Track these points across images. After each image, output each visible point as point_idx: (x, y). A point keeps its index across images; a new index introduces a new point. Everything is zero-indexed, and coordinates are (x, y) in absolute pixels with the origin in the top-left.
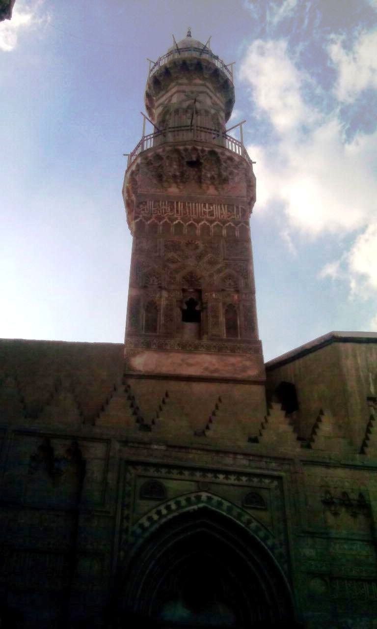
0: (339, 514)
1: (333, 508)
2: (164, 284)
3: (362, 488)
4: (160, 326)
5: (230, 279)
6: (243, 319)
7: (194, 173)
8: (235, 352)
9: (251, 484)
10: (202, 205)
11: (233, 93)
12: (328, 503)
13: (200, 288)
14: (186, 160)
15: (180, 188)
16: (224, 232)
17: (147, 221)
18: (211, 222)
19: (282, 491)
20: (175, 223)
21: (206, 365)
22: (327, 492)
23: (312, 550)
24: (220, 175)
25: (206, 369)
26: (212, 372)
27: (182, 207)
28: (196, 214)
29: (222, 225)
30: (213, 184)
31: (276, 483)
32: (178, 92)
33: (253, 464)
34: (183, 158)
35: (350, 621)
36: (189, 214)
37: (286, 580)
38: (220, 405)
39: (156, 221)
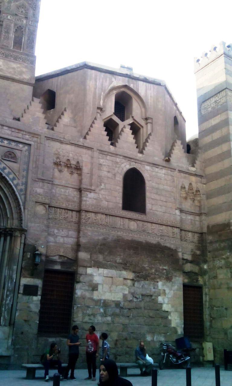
0: (63, 172)
1: (60, 168)
3: (80, 158)
5: (23, 8)
6: (26, 38)
8: (16, 60)
9: (10, 146)
12: (57, 164)
19: (30, 153)
22: (58, 158)
23: (41, 190)
31: (26, 147)
33: (14, 134)
35: (56, 231)
37: (21, 204)
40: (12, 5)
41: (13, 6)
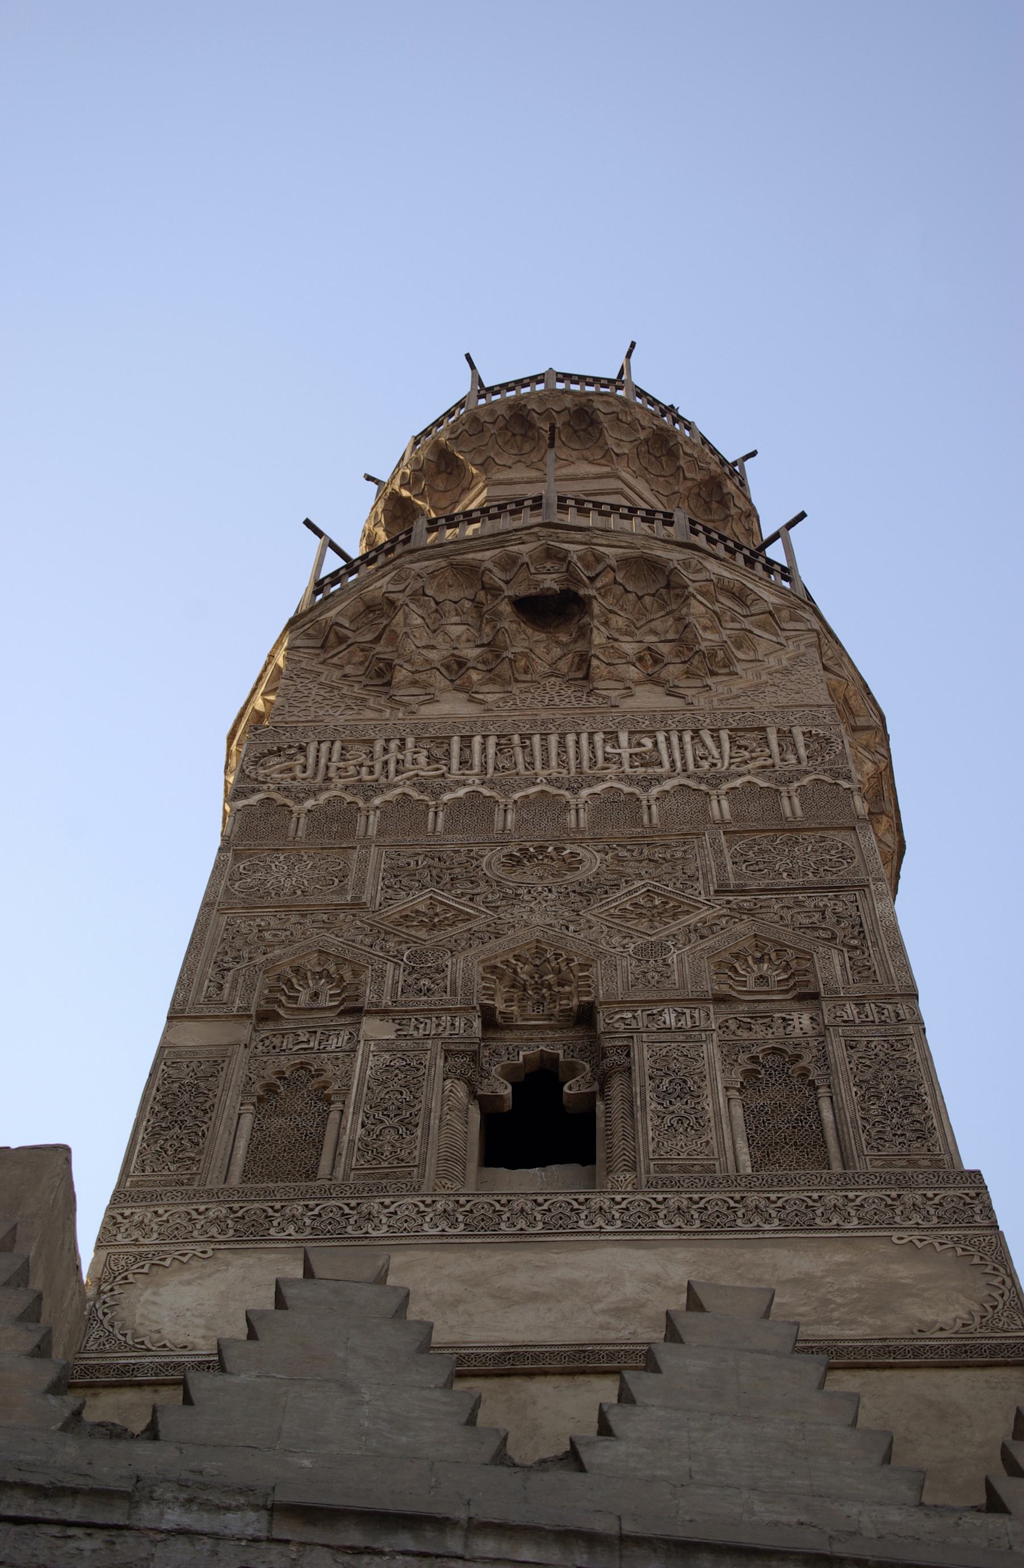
10: (599, 738)
15: (482, 702)
21: (630, 1289)
28: (563, 763)
30: (652, 680)
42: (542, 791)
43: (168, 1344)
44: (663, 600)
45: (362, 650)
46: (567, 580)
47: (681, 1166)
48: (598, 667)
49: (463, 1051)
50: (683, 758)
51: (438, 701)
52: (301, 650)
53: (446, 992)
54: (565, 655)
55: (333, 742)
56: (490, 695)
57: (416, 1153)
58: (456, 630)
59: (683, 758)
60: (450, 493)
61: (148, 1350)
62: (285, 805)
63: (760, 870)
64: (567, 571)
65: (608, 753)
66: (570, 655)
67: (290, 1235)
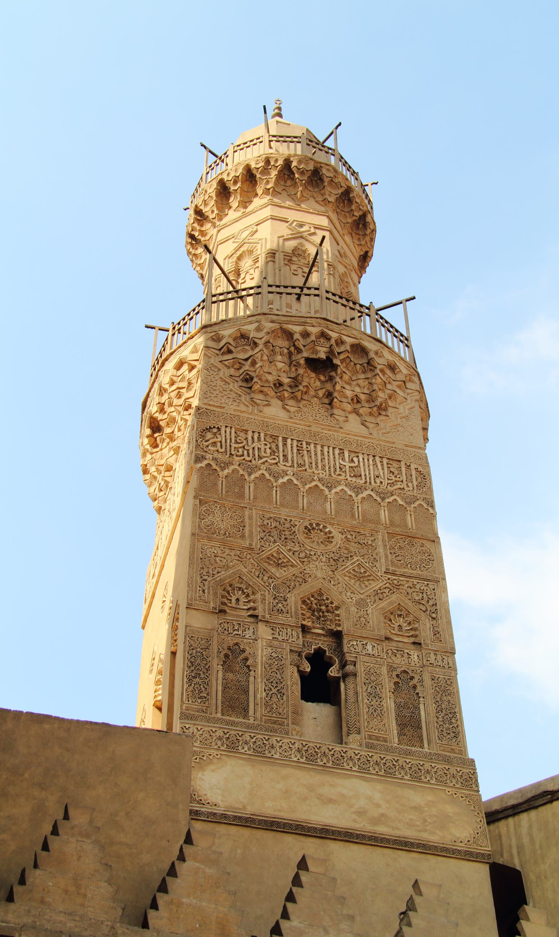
2: (260, 612)
4: (256, 704)
6: (432, 708)
7: (318, 383)
10: (337, 451)
11: (372, 240)
13: (339, 629)
14: (305, 354)
15: (288, 411)
16: (384, 515)
17: (223, 469)
18: (358, 489)
20: (281, 481)
21: (362, 803)
24: (371, 399)
25: (361, 813)
26: (376, 821)
27: (295, 451)
28: (323, 469)
29: (379, 499)
30: (356, 412)
32: (273, 218)
34: (299, 351)
36: (311, 467)
38: (418, 900)
39: (241, 472)
40: (370, 611)
41: (372, 613)
42: (316, 485)
43: (210, 803)
44: (365, 369)
45: (239, 363)
46: (329, 352)
47: (376, 736)
48: (336, 402)
49: (296, 651)
50: (369, 474)
51: (270, 405)
52: (211, 349)
53: (288, 613)
54: (322, 389)
55: (231, 428)
56: (292, 408)
57: (285, 711)
58: (280, 365)
59: (369, 474)
60: (249, 193)
61: (203, 804)
62: (216, 470)
63: (400, 561)
64: (330, 347)
65: (341, 465)
66: (324, 390)
67: (246, 751)
